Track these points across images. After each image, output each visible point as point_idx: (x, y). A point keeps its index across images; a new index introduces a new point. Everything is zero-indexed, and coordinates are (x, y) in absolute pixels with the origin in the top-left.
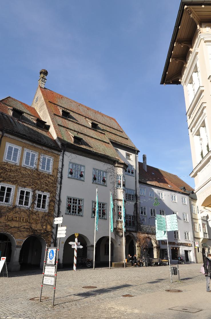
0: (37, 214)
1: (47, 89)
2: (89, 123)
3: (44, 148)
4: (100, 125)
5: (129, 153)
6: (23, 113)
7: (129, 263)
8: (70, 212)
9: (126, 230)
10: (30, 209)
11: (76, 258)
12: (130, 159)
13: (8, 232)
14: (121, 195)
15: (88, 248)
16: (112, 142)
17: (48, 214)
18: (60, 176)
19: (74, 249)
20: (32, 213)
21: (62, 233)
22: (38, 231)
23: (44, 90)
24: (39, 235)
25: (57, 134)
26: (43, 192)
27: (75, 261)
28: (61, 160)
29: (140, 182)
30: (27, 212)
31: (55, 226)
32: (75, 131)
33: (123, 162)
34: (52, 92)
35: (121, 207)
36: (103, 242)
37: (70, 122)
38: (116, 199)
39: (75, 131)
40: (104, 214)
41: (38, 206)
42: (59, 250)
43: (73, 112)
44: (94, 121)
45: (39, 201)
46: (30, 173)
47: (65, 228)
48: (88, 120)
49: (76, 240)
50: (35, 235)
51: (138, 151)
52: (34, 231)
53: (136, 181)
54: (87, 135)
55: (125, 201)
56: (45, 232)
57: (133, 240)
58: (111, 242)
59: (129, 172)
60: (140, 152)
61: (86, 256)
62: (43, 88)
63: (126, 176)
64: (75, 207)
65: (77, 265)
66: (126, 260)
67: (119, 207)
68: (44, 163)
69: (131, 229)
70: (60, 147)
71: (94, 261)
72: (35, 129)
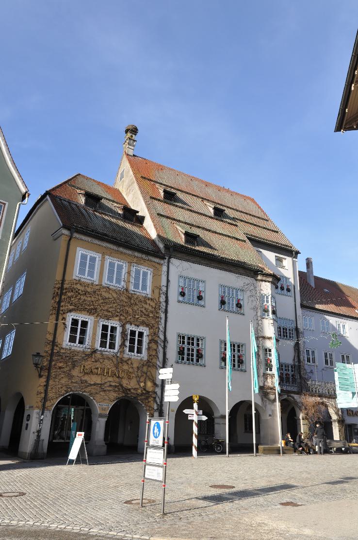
0: (129, 362)
2: (209, 207)
3: (136, 254)
7: (288, 447)
8: (183, 359)
9: (282, 390)
10: (118, 355)
11: (198, 437)
12: (283, 267)
13: (85, 392)
14: (269, 330)
15: (216, 421)
16: (249, 238)
17: (147, 363)
21: (172, 395)
24: (135, 397)
25: (156, 229)
26: (138, 326)
27: (195, 441)
28: (166, 273)
29: (302, 306)
30: (114, 360)
31: (159, 383)
32: (186, 223)
33: (272, 273)
35: (270, 350)
36: (241, 410)
38: (260, 338)
39: (186, 223)
40: (241, 362)
41: (131, 350)
42: (168, 422)
43: (182, 191)
44: (218, 204)
45: (132, 341)
46: (115, 296)
47: (177, 386)
48: (208, 204)
49: (195, 405)
50: (128, 397)
51: (297, 253)
54: (207, 230)
55: (277, 340)
56: (144, 392)
57: (293, 407)
58: (256, 410)
59: (282, 288)
60: (300, 253)
63: (277, 296)
64: (191, 352)
66: (283, 442)
67: (267, 351)
68: (137, 278)
69: (289, 389)
70: (162, 252)
71: (227, 442)
72: (121, 223)
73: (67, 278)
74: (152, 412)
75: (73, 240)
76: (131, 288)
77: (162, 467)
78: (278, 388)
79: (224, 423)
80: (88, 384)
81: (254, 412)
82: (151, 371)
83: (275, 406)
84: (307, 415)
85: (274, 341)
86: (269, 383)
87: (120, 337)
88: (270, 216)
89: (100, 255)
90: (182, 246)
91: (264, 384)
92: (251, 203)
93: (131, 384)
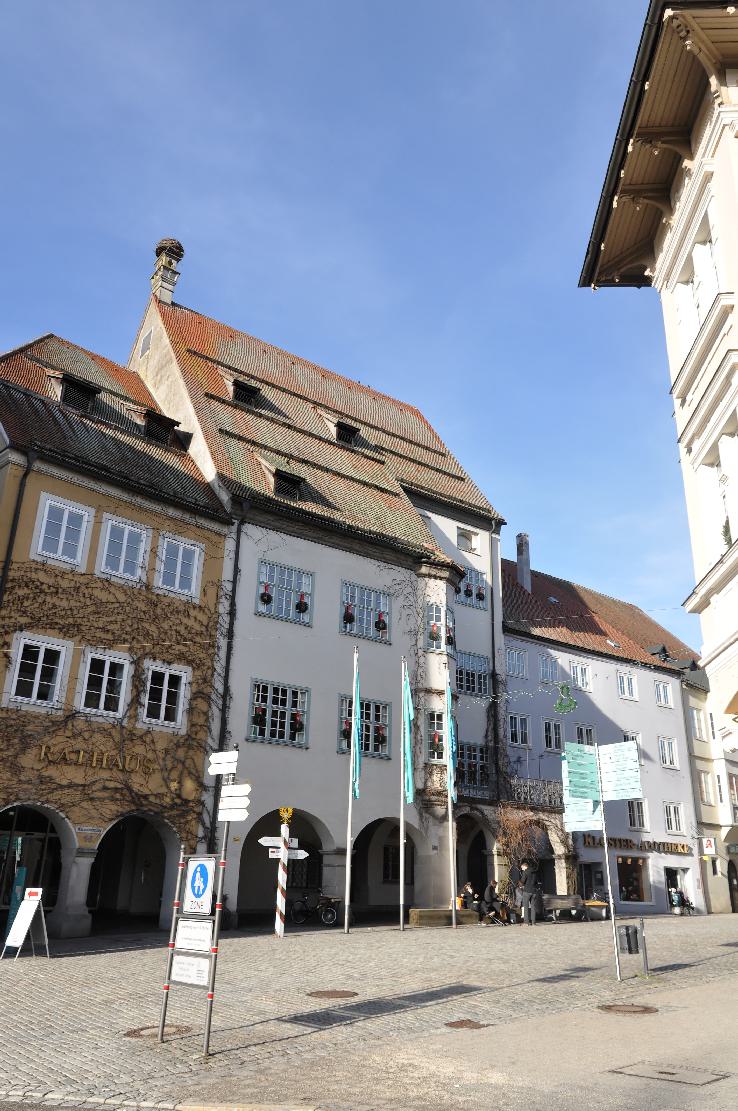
0: (148, 740)
2: (326, 421)
3: (171, 512)
4: (364, 432)
5: (469, 528)
6: (98, 390)
7: (469, 911)
8: (262, 733)
9: (460, 798)
10: (125, 723)
11: (287, 894)
12: (471, 550)
13: (47, 801)
14: (440, 675)
15: (326, 860)
16: (405, 489)
17: (187, 740)
21: (235, 807)
23: (171, 312)
24: (156, 813)
27: (281, 902)
28: (232, 555)
29: (506, 629)
32: (278, 452)
33: (449, 560)
34: (199, 319)
35: (440, 717)
36: (377, 838)
38: (421, 691)
39: (278, 452)
40: (381, 740)
41: (153, 712)
42: (224, 864)
43: (274, 386)
44: (347, 416)
45: (155, 695)
46: (122, 598)
47: (246, 789)
48: (323, 413)
49: (285, 829)
51: (501, 523)
52: (138, 799)
54: (320, 468)
55: (455, 698)
56: (178, 801)
57: (481, 832)
58: (407, 837)
59: (468, 593)
60: (505, 524)
61: (320, 884)
63: (457, 608)
64: (279, 718)
66: (459, 901)
67: (434, 718)
68: (170, 563)
69: (472, 793)
70: (228, 509)
72: (140, 445)
73: (15, 557)
74: (192, 842)
75: (31, 480)
76: (158, 581)
78: (452, 793)
80: (54, 786)
81: (402, 841)
82: (195, 757)
84: (508, 846)
85: (447, 697)
86: (436, 782)
89: (93, 511)
90: (269, 500)
91: (425, 783)
92: (413, 418)
93: (149, 785)
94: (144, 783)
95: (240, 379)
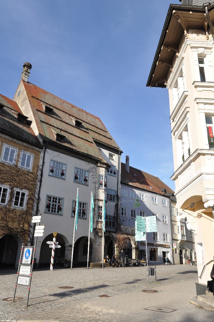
0: (14, 212)
1: (30, 83)
2: (73, 120)
3: (24, 144)
4: (83, 124)
6: (4, 106)
7: (107, 264)
8: (49, 210)
9: (106, 231)
10: (7, 207)
11: (54, 258)
12: (113, 160)
14: (102, 195)
15: (66, 248)
16: (95, 142)
17: (26, 212)
18: (41, 174)
19: (52, 248)
20: (9, 210)
21: (39, 232)
22: (14, 229)
23: (27, 84)
24: (16, 234)
25: (39, 130)
26: (22, 189)
27: (52, 260)
28: (42, 158)
29: (122, 183)
30: (4, 209)
31: (33, 225)
32: (58, 128)
33: (106, 162)
34: (35, 87)
35: (101, 207)
36: (82, 242)
37: (53, 119)
38: (96, 200)
39: (58, 128)
40: (84, 213)
41: (16, 204)
42: (35, 249)
43: (57, 109)
44: (79, 119)
45: (17, 198)
46: (8, 169)
47: (43, 227)
48: (72, 118)
49: (54, 239)
50: (12, 233)
51: (122, 152)
52: (10, 229)
53: (118, 181)
54: (70, 133)
55: (106, 202)
56: (22, 230)
57: (112, 240)
58: (90, 242)
59: (111, 172)
60: (123, 153)
61: (64, 256)
62: (26, 82)
63: (108, 177)
64: (54, 206)
65: (54, 265)
66: (104, 260)
67: (100, 208)
68: (24, 159)
69: (110, 230)
70: (42, 144)
71: (72, 261)
72: (16, 124)
74: (26, 243)
76: (19, 165)
77: (28, 277)
78: (104, 229)
79: (71, 249)
81: (89, 243)
82: (28, 217)
83: (102, 240)
84: (119, 245)
85: (104, 202)
86: (99, 226)
87: (9, 195)
88: (108, 129)
90: (54, 142)
91: (96, 227)
92: (97, 120)
93: (13, 225)
94: (12, 225)
95: (47, 106)
